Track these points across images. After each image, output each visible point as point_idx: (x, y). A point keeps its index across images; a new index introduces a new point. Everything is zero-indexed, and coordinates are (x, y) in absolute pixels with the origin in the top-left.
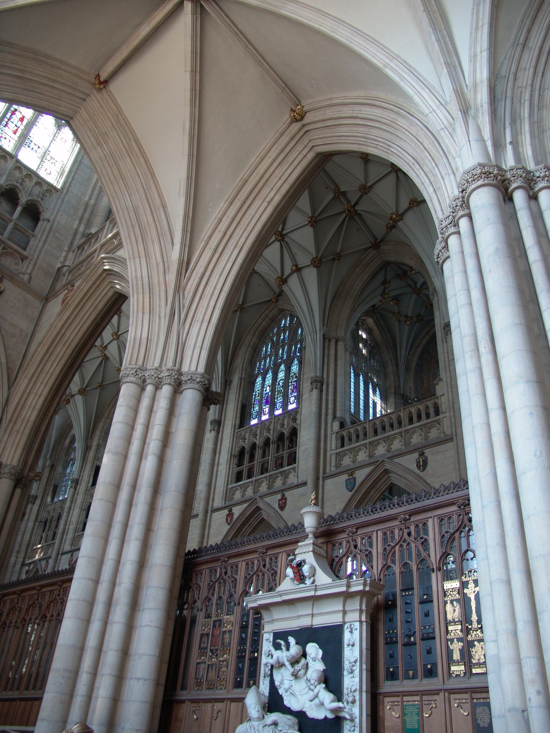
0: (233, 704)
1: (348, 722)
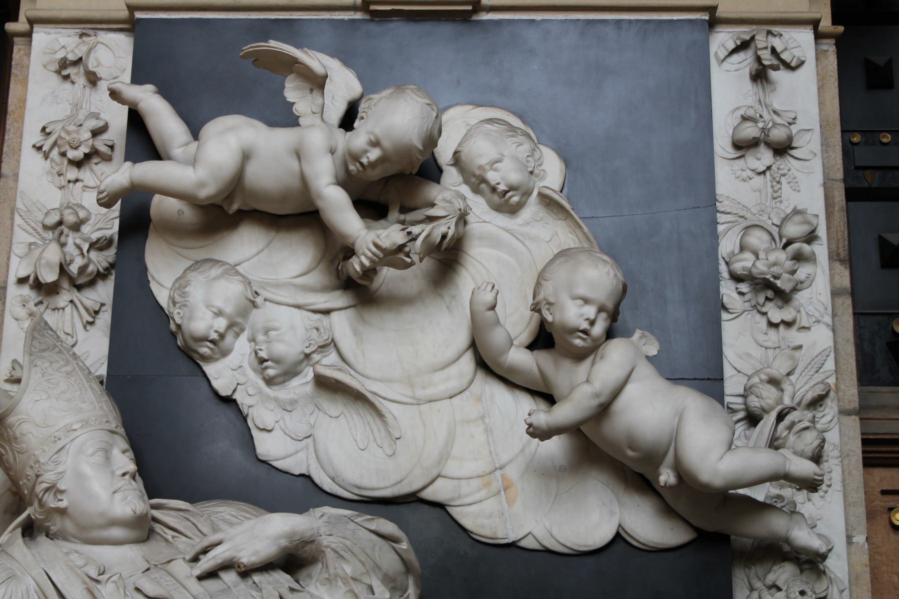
1: (784, 573)
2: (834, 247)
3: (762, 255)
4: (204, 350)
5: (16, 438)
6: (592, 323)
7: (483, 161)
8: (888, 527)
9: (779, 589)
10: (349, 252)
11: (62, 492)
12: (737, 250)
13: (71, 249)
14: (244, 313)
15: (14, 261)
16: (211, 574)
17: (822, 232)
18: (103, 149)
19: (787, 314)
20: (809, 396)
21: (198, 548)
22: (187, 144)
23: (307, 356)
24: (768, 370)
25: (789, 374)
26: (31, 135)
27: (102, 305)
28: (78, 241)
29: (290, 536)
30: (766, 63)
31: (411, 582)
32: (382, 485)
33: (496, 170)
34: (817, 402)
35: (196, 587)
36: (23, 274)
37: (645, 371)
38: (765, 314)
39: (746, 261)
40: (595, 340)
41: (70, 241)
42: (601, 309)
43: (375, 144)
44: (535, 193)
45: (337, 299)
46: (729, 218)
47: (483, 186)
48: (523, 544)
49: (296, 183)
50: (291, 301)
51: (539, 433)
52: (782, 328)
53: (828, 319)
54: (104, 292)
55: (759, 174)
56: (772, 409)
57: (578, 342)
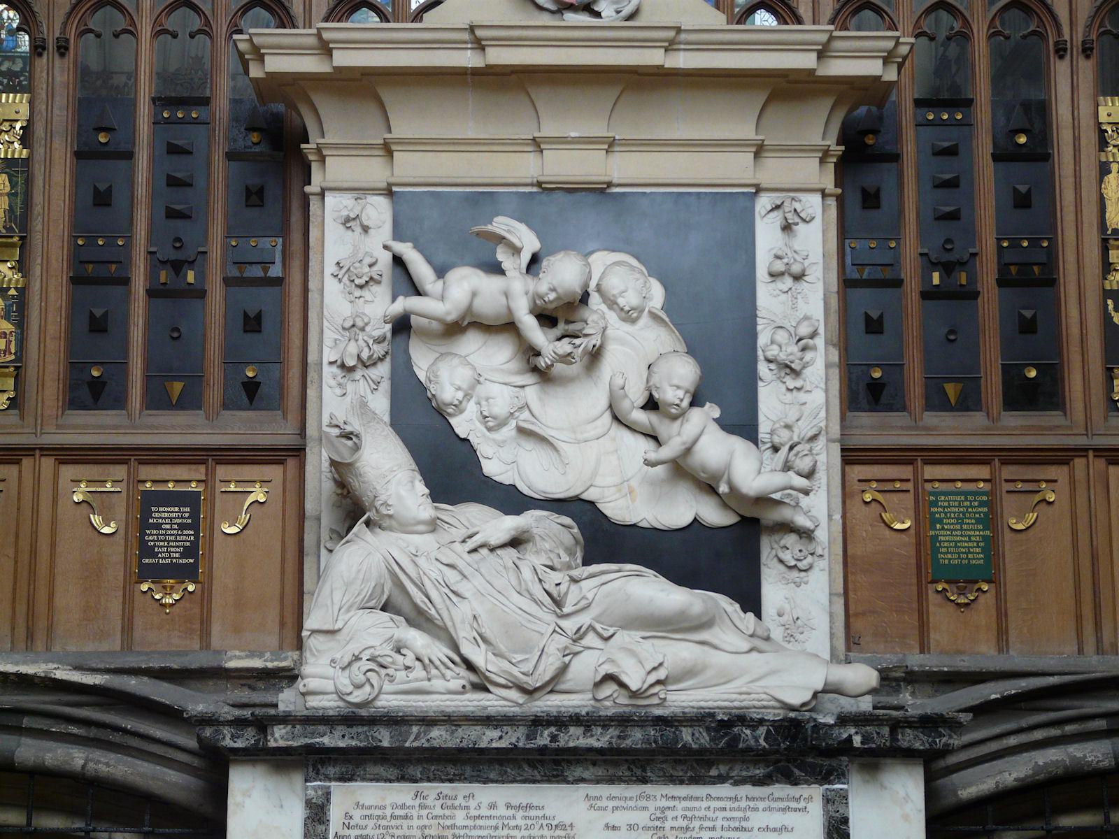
0: (68, 472)
1: (790, 539)
2: (829, 337)
3: (784, 349)
4: (450, 411)
5: (361, 475)
6: (682, 400)
7: (615, 292)
8: (861, 502)
9: (788, 549)
10: (538, 354)
11: (390, 506)
12: (769, 343)
13: (361, 342)
14: (472, 388)
15: (326, 350)
16: (474, 550)
17: (821, 330)
18: (376, 277)
19: (798, 383)
20: (810, 434)
21: (465, 536)
22: (435, 282)
23: (512, 414)
24: (785, 420)
25: (797, 421)
26: (330, 268)
27: (382, 378)
28: (366, 338)
29: (516, 529)
30: (790, 221)
31: (578, 550)
32: (558, 491)
33: (623, 297)
34: (813, 438)
35: (466, 556)
36: (332, 360)
37: (714, 429)
38: (785, 383)
39: (773, 352)
40: (682, 409)
41: (360, 338)
42: (687, 392)
43: (553, 290)
44: (647, 310)
45: (528, 379)
46: (765, 321)
47: (615, 306)
48: (640, 525)
49: (504, 311)
50: (501, 381)
51: (648, 463)
52: (795, 391)
53: (823, 386)
54: (383, 370)
55: (784, 292)
56: (786, 443)
57: (673, 411)
